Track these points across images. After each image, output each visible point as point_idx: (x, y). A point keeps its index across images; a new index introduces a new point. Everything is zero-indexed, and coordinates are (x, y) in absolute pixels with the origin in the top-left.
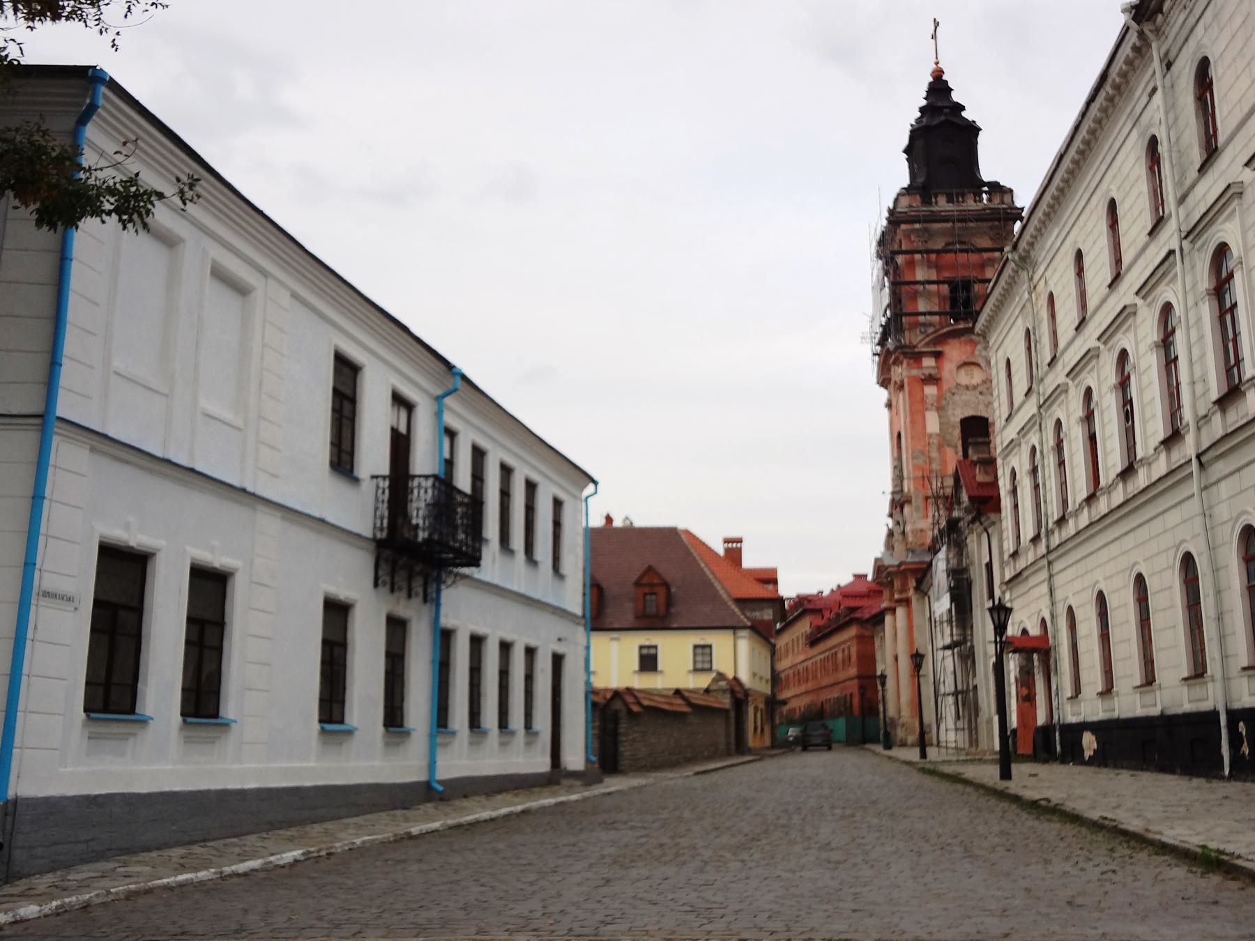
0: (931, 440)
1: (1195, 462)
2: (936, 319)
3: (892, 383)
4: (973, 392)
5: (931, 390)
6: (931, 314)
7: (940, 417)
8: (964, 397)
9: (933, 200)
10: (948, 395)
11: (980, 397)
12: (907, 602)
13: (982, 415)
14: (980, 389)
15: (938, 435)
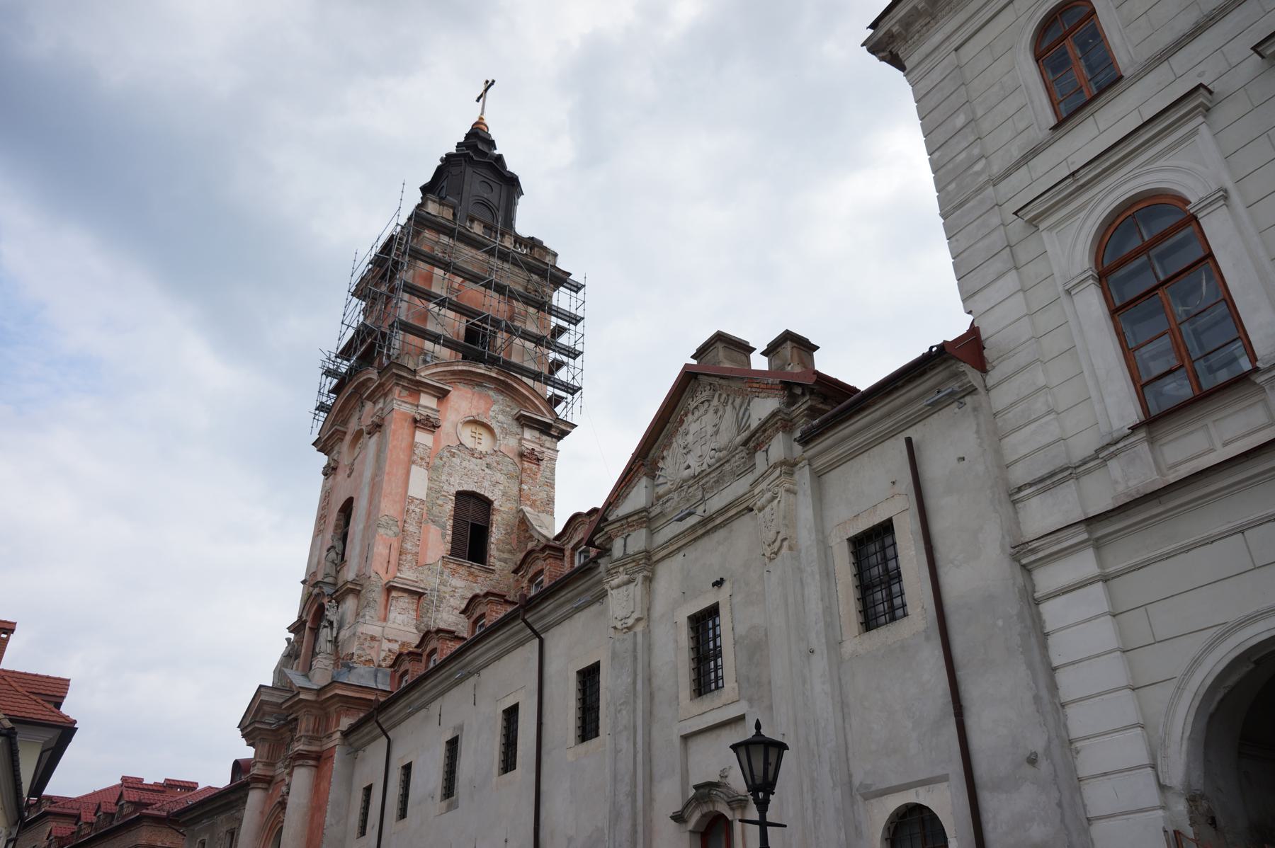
0: (412, 507)
2: (445, 353)
3: (348, 438)
4: (479, 460)
5: (423, 438)
7: (430, 479)
8: (464, 464)
10: (446, 454)
11: (487, 470)
12: (319, 760)
13: (486, 495)
14: (488, 459)
15: (422, 502)
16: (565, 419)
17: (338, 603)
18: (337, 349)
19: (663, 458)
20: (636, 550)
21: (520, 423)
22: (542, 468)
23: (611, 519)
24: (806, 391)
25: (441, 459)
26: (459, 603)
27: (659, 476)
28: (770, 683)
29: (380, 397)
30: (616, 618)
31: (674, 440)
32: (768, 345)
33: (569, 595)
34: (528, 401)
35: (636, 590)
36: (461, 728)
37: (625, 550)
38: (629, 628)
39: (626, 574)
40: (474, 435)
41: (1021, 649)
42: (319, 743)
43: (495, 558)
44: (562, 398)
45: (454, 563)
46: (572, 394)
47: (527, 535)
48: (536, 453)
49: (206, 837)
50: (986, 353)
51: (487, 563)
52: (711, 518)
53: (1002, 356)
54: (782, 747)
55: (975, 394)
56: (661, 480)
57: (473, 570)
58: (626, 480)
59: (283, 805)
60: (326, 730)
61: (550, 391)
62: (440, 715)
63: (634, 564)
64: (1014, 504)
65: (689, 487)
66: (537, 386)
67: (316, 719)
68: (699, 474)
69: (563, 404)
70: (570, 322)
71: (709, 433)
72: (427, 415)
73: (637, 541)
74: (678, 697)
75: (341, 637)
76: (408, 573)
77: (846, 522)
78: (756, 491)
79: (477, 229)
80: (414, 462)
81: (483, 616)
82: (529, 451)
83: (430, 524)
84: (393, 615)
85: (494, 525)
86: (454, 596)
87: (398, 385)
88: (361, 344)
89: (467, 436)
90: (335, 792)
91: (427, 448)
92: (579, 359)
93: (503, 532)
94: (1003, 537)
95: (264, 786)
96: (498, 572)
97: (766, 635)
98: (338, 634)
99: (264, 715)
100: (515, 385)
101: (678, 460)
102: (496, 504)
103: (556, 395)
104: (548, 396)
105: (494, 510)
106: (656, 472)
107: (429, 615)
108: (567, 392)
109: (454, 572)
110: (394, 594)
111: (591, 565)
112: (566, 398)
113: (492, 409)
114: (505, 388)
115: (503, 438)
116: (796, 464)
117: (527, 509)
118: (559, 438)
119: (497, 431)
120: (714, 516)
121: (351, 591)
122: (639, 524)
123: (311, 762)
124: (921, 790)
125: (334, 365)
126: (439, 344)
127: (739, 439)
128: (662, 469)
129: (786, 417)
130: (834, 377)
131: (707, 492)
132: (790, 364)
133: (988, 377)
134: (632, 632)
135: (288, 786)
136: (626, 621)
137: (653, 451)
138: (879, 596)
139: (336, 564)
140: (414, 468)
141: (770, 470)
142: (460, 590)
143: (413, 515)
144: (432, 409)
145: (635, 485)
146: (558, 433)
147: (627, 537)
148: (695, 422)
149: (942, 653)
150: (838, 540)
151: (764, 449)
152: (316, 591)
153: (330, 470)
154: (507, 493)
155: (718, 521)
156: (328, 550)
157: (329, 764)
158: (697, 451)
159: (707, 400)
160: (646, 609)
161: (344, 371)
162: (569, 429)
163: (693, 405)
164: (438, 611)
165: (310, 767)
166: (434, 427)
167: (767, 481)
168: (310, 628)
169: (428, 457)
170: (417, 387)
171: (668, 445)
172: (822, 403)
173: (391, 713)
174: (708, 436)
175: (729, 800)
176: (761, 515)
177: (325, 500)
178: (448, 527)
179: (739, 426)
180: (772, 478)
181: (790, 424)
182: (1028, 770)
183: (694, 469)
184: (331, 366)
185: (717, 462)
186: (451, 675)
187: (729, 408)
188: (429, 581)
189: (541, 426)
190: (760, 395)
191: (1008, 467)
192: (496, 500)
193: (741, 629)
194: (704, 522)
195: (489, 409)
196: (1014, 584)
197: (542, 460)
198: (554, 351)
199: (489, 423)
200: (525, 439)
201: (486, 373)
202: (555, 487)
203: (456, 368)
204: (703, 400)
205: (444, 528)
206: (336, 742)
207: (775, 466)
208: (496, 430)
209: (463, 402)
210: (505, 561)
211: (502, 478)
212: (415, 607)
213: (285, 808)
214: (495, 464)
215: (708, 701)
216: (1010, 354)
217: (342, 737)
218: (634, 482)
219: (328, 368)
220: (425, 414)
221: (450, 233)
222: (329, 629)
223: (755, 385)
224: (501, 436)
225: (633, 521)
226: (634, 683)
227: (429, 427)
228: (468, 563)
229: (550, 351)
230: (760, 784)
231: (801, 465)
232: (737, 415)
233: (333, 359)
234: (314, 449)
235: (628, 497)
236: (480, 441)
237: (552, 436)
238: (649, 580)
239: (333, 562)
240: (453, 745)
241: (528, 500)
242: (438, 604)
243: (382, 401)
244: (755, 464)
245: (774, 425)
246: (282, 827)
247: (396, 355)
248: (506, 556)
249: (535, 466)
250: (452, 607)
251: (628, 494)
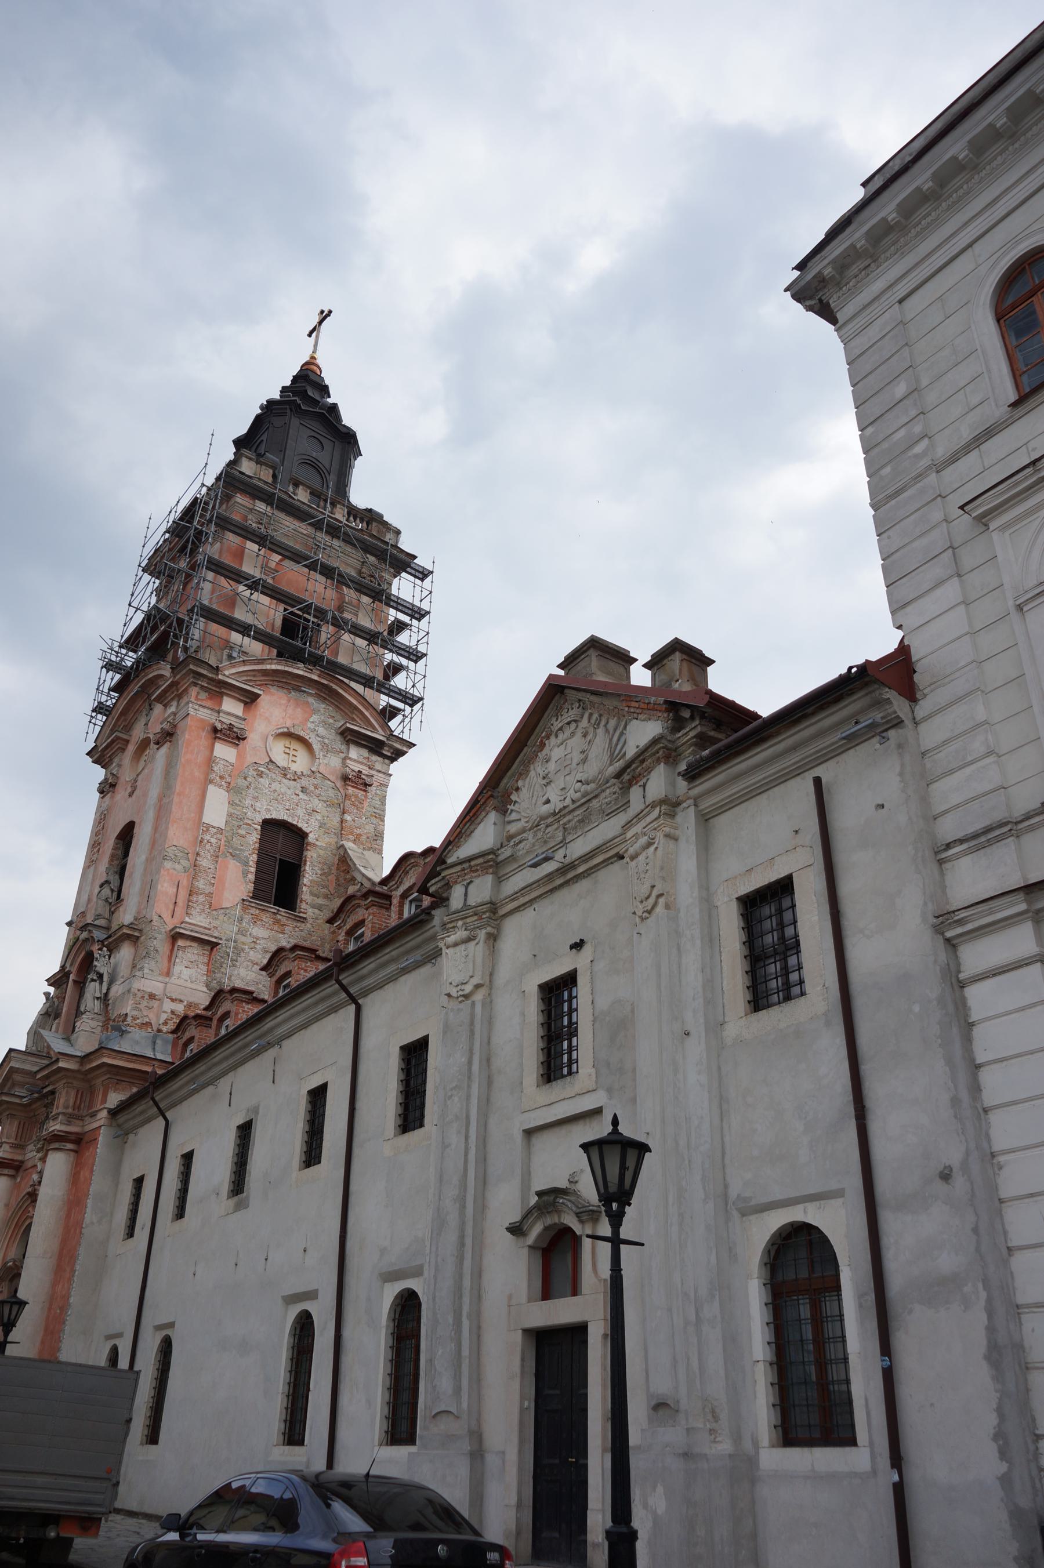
0: (207, 837)
2: (256, 648)
3: (131, 748)
5: (223, 751)
7: (231, 803)
8: (274, 786)
10: (252, 772)
11: (302, 796)
13: (300, 825)
14: (304, 782)
15: (220, 830)
16: (400, 736)
17: (110, 951)
18: (122, 636)
19: (517, 789)
20: (479, 900)
21: (345, 738)
22: (370, 795)
23: (450, 861)
24: (695, 714)
25: (245, 778)
26: (260, 956)
27: (512, 811)
28: (634, 1070)
29: (172, 699)
30: (451, 983)
31: (532, 767)
32: (652, 656)
33: (393, 953)
34: (356, 712)
35: (477, 950)
36: (256, 1110)
37: (465, 900)
38: (466, 997)
39: (466, 930)
40: (287, 751)
41: (939, 1041)
42: (81, 1123)
43: (307, 903)
44: (399, 710)
45: (256, 908)
46: (411, 706)
47: (348, 876)
48: (363, 776)
50: (917, 678)
51: (297, 910)
52: (572, 866)
53: (935, 682)
54: (643, 1148)
55: (901, 728)
56: (514, 816)
57: (279, 917)
58: (471, 814)
59: (32, 1197)
60: (90, 1107)
61: (384, 700)
62: (231, 1094)
63: (475, 918)
64: (941, 864)
65: (547, 826)
66: (369, 693)
67: (78, 1091)
68: (561, 810)
69: (399, 718)
70: (412, 617)
71: (575, 761)
72: (231, 724)
73: (482, 889)
74: (522, 1083)
76: (199, 918)
77: (736, 877)
78: (629, 835)
79: (302, 496)
80: (211, 782)
81: (288, 974)
82: (354, 774)
84: (177, 969)
85: (308, 863)
86: (255, 948)
87: (195, 684)
88: (152, 633)
89: (278, 751)
90: (98, 1183)
91: (228, 764)
92: (422, 662)
93: (319, 872)
94: (925, 904)
95: (11, 1172)
96: (310, 921)
97: (633, 1011)
98: (108, 989)
99: (13, 1085)
100: (341, 691)
101: (535, 793)
102: (311, 838)
103: (391, 706)
104: (381, 707)
105: (308, 844)
106: (508, 806)
107: (223, 970)
108: (405, 703)
109: (255, 920)
110: (180, 943)
111: (423, 917)
112: (404, 710)
113: (311, 720)
114: (328, 695)
115: (324, 756)
116: (678, 804)
117: (349, 845)
118: (393, 760)
119: (316, 746)
120: (576, 863)
121: (128, 937)
122: (484, 869)
123: (70, 1146)
124: (811, 1207)
125: (117, 657)
126: (249, 636)
127: (612, 770)
128: (516, 802)
129: (670, 746)
130: (730, 698)
131: (570, 833)
132: (677, 681)
133: (918, 707)
134: (469, 1002)
135: (41, 1173)
136: (463, 987)
137: (505, 781)
138: (771, 969)
139: (110, 904)
140: (211, 788)
141: (647, 810)
142: (262, 942)
143: (208, 847)
144: (237, 717)
145: (482, 820)
146: (392, 753)
147: (469, 884)
148: (558, 746)
149: (844, 1042)
150: (726, 899)
151: (641, 783)
152: (84, 935)
153: (108, 786)
154: (325, 824)
155: (581, 869)
156: (101, 886)
157: (91, 1149)
158: (560, 782)
159: (575, 721)
160: (488, 973)
161: (129, 664)
162: (405, 749)
163: (557, 725)
164: (234, 966)
165: (66, 1152)
166: (238, 739)
167: (643, 824)
168: (74, 981)
169: (230, 776)
170: (219, 689)
171: (523, 774)
172: (714, 730)
173: (171, 1089)
174: (574, 764)
175: (578, 1211)
176: (633, 864)
177: (100, 823)
178: (251, 863)
179: (612, 754)
180: (649, 819)
181: (674, 754)
182: (940, 1187)
183: (556, 804)
184: (113, 658)
185: (583, 796)
186: (247, 1045)
187: (601, 731)
188: (224, 929)
189: (371, 743)
190: (640, 716)
191: (935, 819)
192: (311, 832)
193: (603, 1003)
194: (563, 870)
195: (307, 720)
196: (935, 961)
197: (370, 785)
198: (391, 651)
199: (307, 737)
200: (350, 759)
201: (306, 674)
202: (385, 818)
203: (268, 667)
204: (569, 719)
205: (246, 863)
206: (102, 1122)
207: (653, 805)
208: (314, 746)
210: (320, 908)
213: (36, 1201)
214: (312, 788)
215: (559, 1089)
216: (947, 680)
217: (109, 1117)
218: (481, 817)
219: (110, 660)
220: (228, 722)
221: (268, 498)
222: (97, 984)
223: (634, 704)
224: (321, 753)
225: (477, 865)
226: (470, 1062)
227: (233, 738)
228: (273, 909)
229: (386, 651)
230: (614, 1193)
231: (685, 805)
232: (611, 740)
233: (116, 649)
235: (473, 835)
236: (294, 759)
237: (385, 757)
238: (493, 938)
239: (106, 900)
240: (245, 1131)
241: (352, 833)
242: (234, 958)
243: (174, 703)
244: (629, 801)
245: (654, 754)
246: (30, 1224)
247: (194, 647)
248: (321, 901)
249: (362, 792)
250: (252, 962)
251: (472, 832)
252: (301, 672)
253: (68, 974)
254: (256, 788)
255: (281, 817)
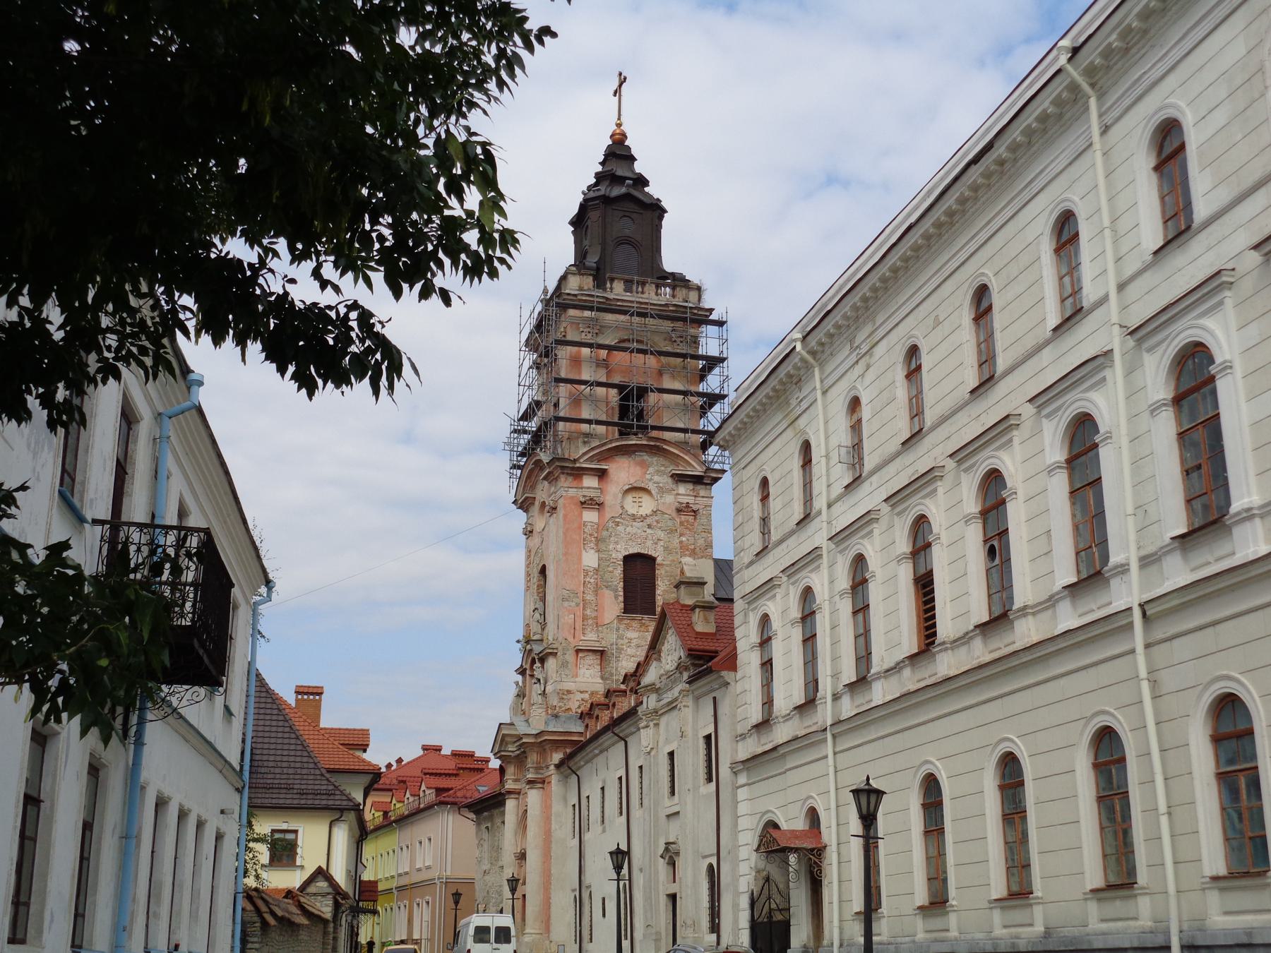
0: (588, 579)
1: (1137, 614)
2: (601, 429)
3: (537, 503)
5: (590, 516)
6: (599, 422)
8: (629, 529)
9: (608, 285)
10: (611, 524)
11: (649, 531)
13: (650, 553)
25: (607, 530)
40: (635, 500)
49: (489, 825)
75: (547, 692)
76: (590, 635)
83: (605, 589)
87: (563, 473)
93: (668, 583)
99: (507, 744)
102: (659, 560)
109: (628, 627)
110: (580, 655)
115: (661, 497)
121: (551, 653)
143: (589, 586)
188: (608, 639)
205: (616, 591)
208: (653, 492)
209: (623, 472)
211: (661, 534)
212: (599, 662)
214: (655, 524)
234: (514, 507)
236: (640, 504)
241: (687, 550)
252: (634, 442)
253: (525, 669)
254: (616, 535)
255: (636, 552)
